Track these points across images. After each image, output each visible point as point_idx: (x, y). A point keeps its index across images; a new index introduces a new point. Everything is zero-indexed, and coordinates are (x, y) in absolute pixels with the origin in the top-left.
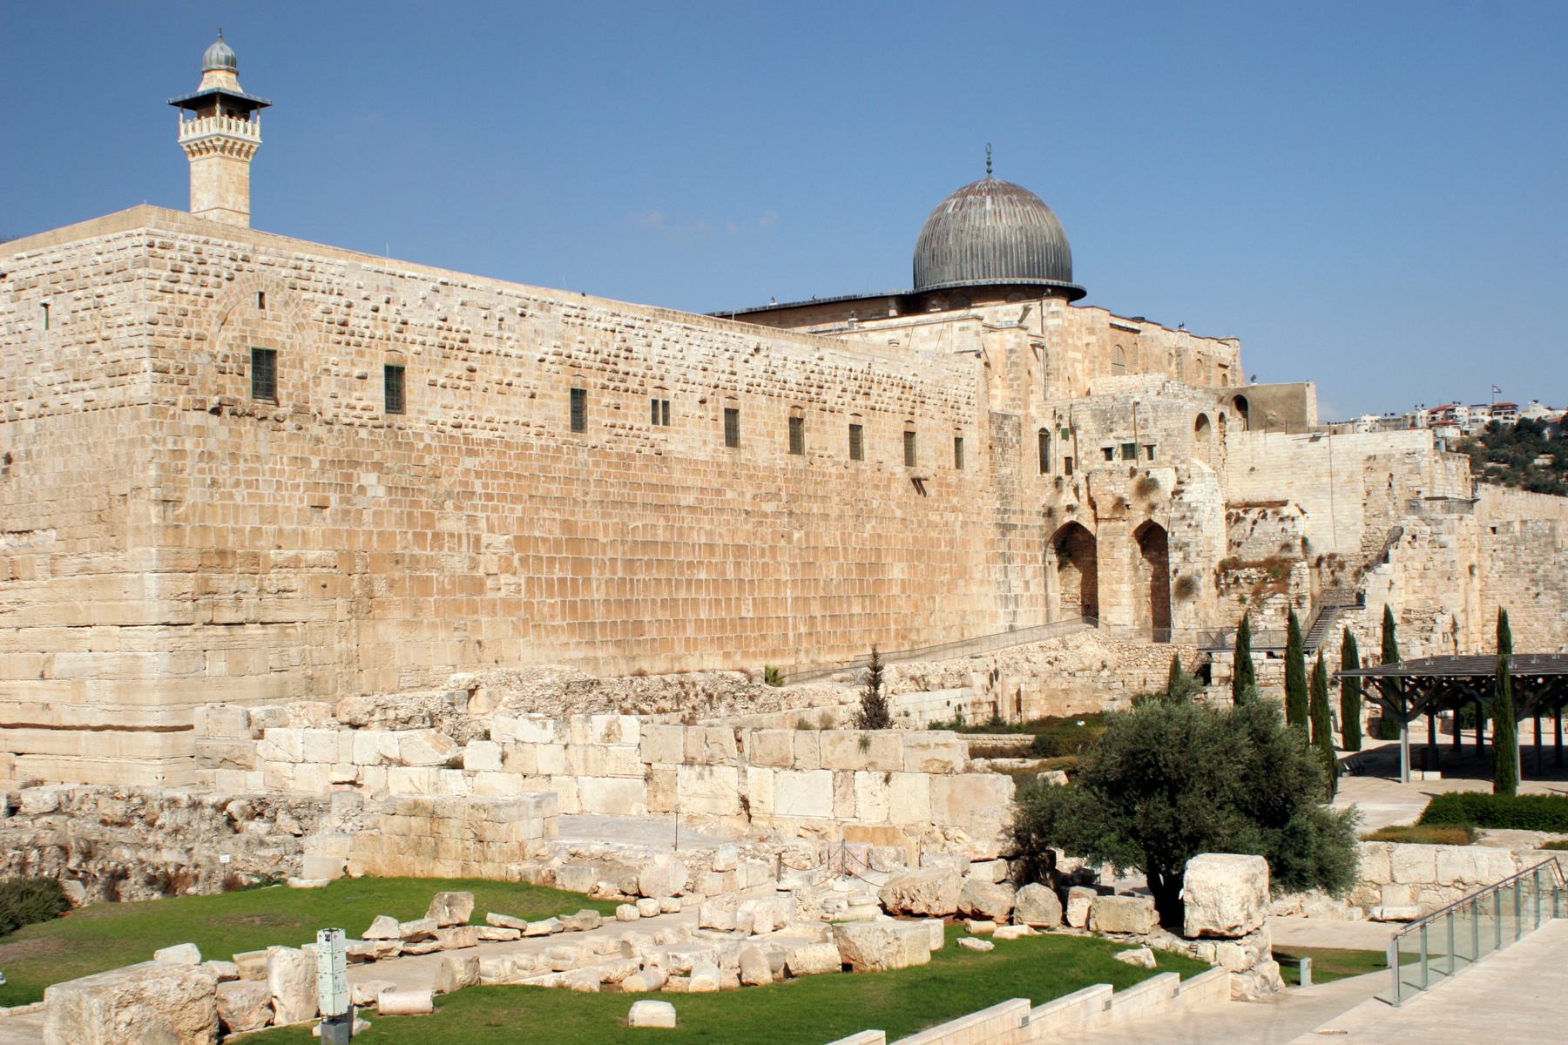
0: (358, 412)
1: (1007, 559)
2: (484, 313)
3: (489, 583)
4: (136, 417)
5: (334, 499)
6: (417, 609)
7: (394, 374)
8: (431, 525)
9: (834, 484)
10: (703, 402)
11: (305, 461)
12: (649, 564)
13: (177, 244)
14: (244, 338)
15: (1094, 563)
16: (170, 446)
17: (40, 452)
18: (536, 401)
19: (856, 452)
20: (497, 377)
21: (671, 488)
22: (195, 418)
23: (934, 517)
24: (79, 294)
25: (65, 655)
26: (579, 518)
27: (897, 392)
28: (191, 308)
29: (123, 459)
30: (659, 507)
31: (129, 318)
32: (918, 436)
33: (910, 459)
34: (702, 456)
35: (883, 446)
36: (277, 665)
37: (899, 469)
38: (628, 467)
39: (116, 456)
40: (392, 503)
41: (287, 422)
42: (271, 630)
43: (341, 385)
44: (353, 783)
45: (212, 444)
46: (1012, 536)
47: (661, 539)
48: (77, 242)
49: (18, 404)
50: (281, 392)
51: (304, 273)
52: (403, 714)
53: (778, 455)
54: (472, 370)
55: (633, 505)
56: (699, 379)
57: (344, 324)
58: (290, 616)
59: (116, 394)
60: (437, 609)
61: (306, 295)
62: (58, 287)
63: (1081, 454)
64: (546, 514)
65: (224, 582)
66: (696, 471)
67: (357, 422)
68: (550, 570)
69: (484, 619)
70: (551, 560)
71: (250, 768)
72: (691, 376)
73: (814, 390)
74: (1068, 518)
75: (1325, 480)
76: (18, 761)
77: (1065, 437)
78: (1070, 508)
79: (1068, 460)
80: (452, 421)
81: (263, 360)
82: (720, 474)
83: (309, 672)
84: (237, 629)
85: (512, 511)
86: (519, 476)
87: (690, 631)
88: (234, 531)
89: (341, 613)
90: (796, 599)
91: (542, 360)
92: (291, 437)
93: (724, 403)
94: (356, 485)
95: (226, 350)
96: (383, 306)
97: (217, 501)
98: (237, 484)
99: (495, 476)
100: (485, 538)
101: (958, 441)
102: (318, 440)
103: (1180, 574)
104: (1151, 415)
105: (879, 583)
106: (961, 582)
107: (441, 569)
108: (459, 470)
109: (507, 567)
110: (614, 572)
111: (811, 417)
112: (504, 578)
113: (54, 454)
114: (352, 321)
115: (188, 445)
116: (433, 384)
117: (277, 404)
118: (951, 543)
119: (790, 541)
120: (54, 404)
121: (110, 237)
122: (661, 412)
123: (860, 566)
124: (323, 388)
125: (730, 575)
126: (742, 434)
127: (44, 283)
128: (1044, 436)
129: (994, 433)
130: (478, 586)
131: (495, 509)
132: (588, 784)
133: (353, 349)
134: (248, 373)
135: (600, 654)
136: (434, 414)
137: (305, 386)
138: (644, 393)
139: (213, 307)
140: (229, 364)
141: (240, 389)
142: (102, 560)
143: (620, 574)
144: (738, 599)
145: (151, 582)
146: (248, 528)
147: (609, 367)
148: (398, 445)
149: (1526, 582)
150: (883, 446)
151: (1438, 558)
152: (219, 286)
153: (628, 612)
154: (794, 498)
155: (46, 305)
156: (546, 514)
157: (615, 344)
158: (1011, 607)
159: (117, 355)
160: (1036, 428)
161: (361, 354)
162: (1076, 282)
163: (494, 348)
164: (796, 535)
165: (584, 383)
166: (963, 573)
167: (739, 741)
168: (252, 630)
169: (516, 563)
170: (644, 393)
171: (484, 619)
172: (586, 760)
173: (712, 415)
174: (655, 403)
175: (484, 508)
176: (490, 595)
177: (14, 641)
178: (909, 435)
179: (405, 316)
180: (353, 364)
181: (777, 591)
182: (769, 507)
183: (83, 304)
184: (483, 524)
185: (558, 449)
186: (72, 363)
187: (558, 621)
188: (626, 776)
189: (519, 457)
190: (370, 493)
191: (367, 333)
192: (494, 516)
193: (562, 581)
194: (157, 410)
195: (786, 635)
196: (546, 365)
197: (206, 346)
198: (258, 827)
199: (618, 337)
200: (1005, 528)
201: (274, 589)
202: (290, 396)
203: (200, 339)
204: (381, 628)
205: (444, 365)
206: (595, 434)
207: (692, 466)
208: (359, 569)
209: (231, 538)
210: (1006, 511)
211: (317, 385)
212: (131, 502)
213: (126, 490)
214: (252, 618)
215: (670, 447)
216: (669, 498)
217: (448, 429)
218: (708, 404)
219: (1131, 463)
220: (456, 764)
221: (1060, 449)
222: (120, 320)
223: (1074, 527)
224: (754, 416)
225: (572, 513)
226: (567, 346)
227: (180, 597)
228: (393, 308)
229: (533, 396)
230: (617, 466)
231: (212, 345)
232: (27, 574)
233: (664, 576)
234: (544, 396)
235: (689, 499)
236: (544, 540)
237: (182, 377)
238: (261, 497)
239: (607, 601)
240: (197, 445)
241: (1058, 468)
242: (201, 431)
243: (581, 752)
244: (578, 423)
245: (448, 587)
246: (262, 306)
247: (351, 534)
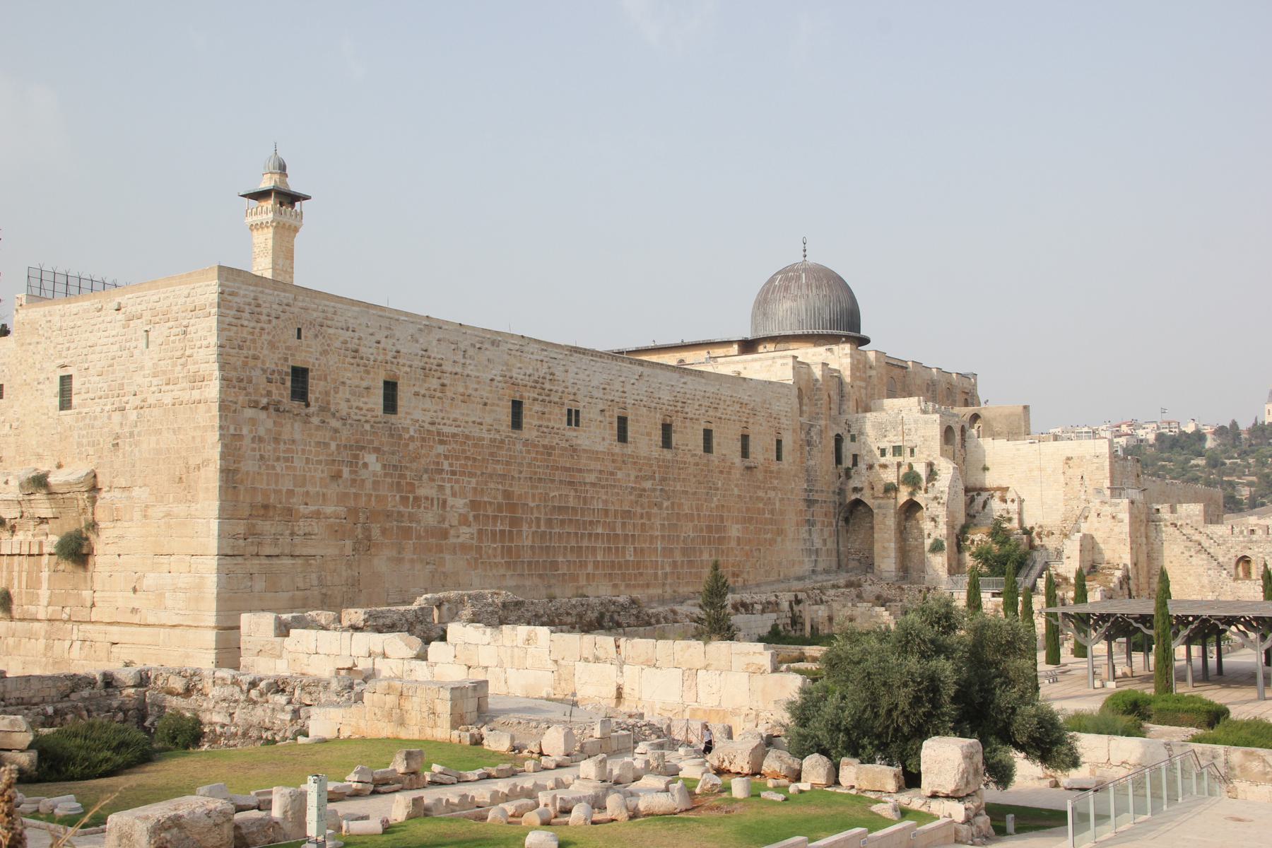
0: (364, 412)
1: (811, 523)
2: (453, 346)
3: (452, 532)
4: (209, 411)
5: (346, 472)
6: (401, 549)
7: (390, 388)
8: (413, 491)
9: (692, 469)
10: (602, 411)
11: (326, 445)
12: (563, 522)
13: (242, 292)
14: (286, 359)
15: (872, 528)
16: (232, 431)
17: (139, 434)
18: (488, 408)
19: (708, 448)
20: (461, 390)
21: (580, 471)
22: (249, 413)
23: (761, 493)
25: (152, 575)
26: (517, 490)
27: (737, 407)
28: (250, 337)
29: (198, 440)
30: (571, 483)
31: (205, 343)
32: (751, 438)
33: (745, 453)
34: (601, 449)
35: (726, 445)
36: (301, 585)
37: (737, 459)
38: (550, 454)
40: (386, 475)
41: (315, 420)
42: (299, 561)
43: (353, 394)
44: (350, 669)
45: (262, 432)
46: (816, 508)
47: (571, 505)
49: (125, 399)
50: (311, 397)
51: (329, 315)
52: (388, 621)
53: (653, 448)
54: (443, 385)
55: (553, 481)
56: (601, 395)
57: (356, 351)
58: (312, 552)
59: (196, 394)
60: (415, 549)
61: (331, 331)
62: (157, 319)
63: (864, 452)
64: (492, 486)
65: (266, 527)
66: (597, 459)
67: (363, 419)
68: (495, 524)
69: (447, 557)
70: (495, 517)
71: (280, 657)
72: (595, 394)
73: (680, 404)
74: (853, 497)
75: (1036, 473)
76: (115, 649)
77: (853, 439)
78: (856, 490)
79: (855, 457)
80: (428, 420)
81: (300, 376)
82: (613, 461)
83: (324, 591)
84: (275, 561)
85: (469, 482)
86: (475, 459)
87: (590, 569)
88: (275, 491)
89: (348, 550)
90: (664, 549)
91: (492, 380)
92: (318, 428)
93: (617, 412)
94: (361, 463)
95: (273, 367)
96: (383, 340)
97: (263, 470)
98: (278, 459)
99: (457, 458)
100: (451, 501)
101: (779, 442)
102: (336, 431)
103: (933, 536)
104: (912, 426)
105: (721, 540)
106: (779, 539)
107: (418, 522)
108: (434, 452)
109: (464, 521)
110: (538, 526)
111: (677, 424)
112: (464, 529)
114: (363, 350)
115: (245, 431)
116: (416, 394)
117: (308, 405)
118: (772, 512)
119: (661, 508)
120: (151, 400)
122: (573, 417)
123: (709, 528)
124: (340, 395)
125: (619, 532)
126: (629, 434)
127: (147, 316)
128: (839, 440)
129: (803, 436)
130: (444, 534)
131: (457, 482)
132: (512, 674)
133: (362, 369)
134: (289, 384)
135: (528, 583)
136: (418, 415)
137: (327, 393)
138: (563, 404)
139: (265, 337)
140: (276, 376)
141: (282, 393)
142: (180, 509)
143: (543, 529)
144: (624, 548)
145: (214, 525)
146: (284, 489)
147: (538, 386)
148: (391, 436)
149: (1182, 548)
150: (726, 445)
151: (1117, 530)
152: (270, 321)
153: (548, 554)
154: (663, 479)
156: (492, 486)
157: (543, 370)
158: (813, 557)
160: (832, 434)
161: (368, 372)
162: (864, 332)
163: (459, 370)
164: (666, 504)
165: (521, 396)
166: (780, 532)
167: (618, 647)
168: (287, 561)
169: (471, 519)
170: (563, 404)
171: (447, 557)
172: (512, 657)
173: (608, 419)
174: (570, 411)
175: (450, 480)
176: (452, 540)
177: (116, 564)
178: (745, 439)
179: (399, 347)
180: (362, 379)
181: (651, 543)
182: (648, 485)
183: (175, 331)
184: (448, 491)
185: (502, 442)
186: (164, 372)
187: (499, 559)
188: (539, 669)
189: (475, 446)
190: (371, 468)
191: (372, 358)
192: (457, 487)
193: (503, 532)
194: (224, 407)
195: (656, 574)
196: (495, 383)
197: (259, 364)
198: (281, 699)
199: (545, 365)
200: (810, 503)
201: (301, 533)
202: (317, 399)
203: (255, 358)
204: (376, 561)
205: (424, 381)
206: (529, 432)
207: (594, 455)
208: (361, 520)
209: (272, 496)
210: (811, 491)
211: (336, 393)
212: (202, 470)
214: (286, 552)
215: (579, 442)
216: (578, 477)
217: (427, 426)
218: (607, 414)
219: (900, 459)
220: (422, 656)
221: (849, 448)
222: (198, 344)
223: (858, 502)
224: (638, 421)
225: (511, 485)
226: (510, 371)
227: (235, 537)
228: (391, 341)
229: (485, 404)
230: (542, 454)
231: (263, 362)
232: (128, 517)
233: (572, 530)
234: (493, 405)
235: (591, 478)
236: (490, 503)
237: (242, 385)
238: (295, 468)
239: (532, 547)
240: (251, 431)
241: (847, 462)
242: (253, 421)
243: (509, 651)
244: (517, 423)
245: (423, 534)
246: (299, 337)
247: (356, 496)
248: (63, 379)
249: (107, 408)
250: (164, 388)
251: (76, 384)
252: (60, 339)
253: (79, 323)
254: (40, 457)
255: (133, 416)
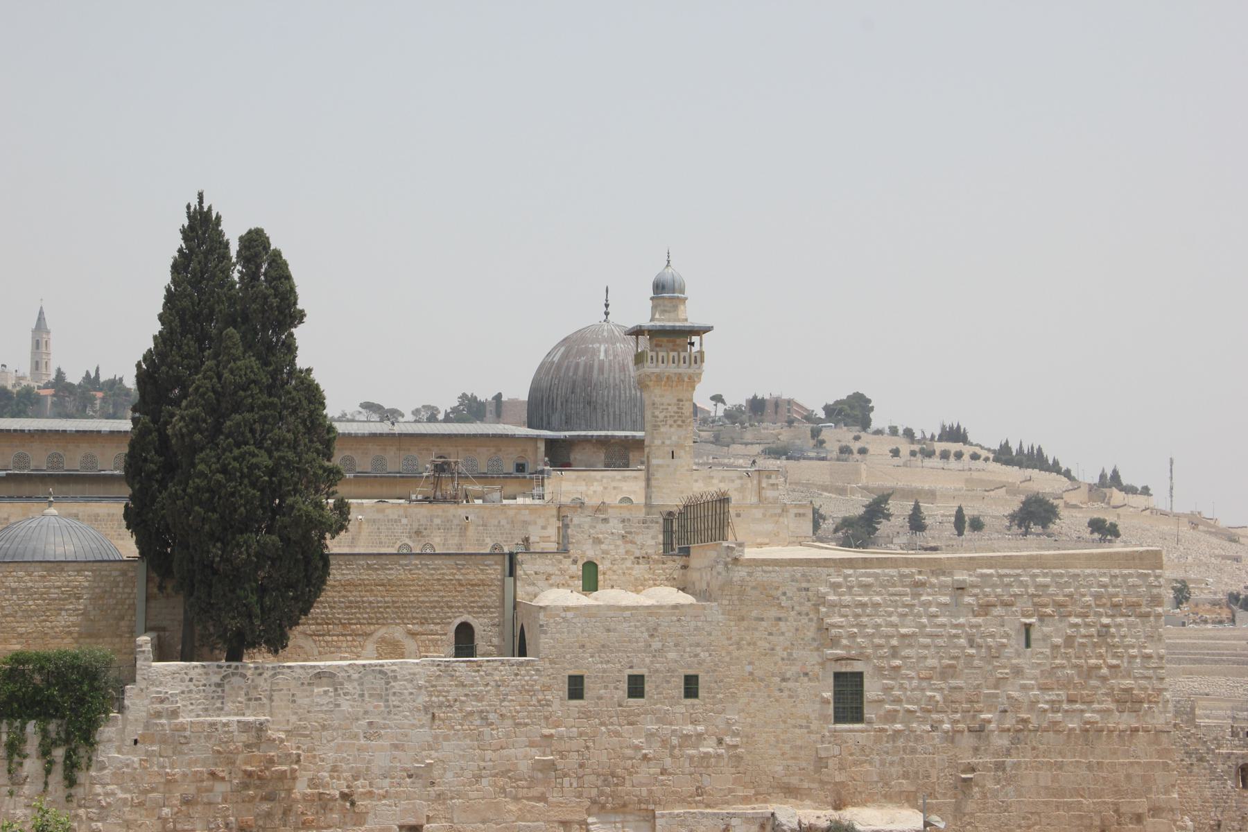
17: (1016, 766)
24: (1078, 620)
39: (1128, 777)
48: (1072, 571)
62: (1049, 611)
113: (1038, 769)
121: (1117, 571)
155: (1028, 627)
159: (1128, 683)
186: (1067, 684)
213: (1142, 805)
222: (1134, 652)
248: (837, 676)
249: (946, 726)
250: (1065, 706)
251: (871, 690)
252: (837, 619)
253: (878, 599)
254: (791, 792)
255: (1004, 742)
